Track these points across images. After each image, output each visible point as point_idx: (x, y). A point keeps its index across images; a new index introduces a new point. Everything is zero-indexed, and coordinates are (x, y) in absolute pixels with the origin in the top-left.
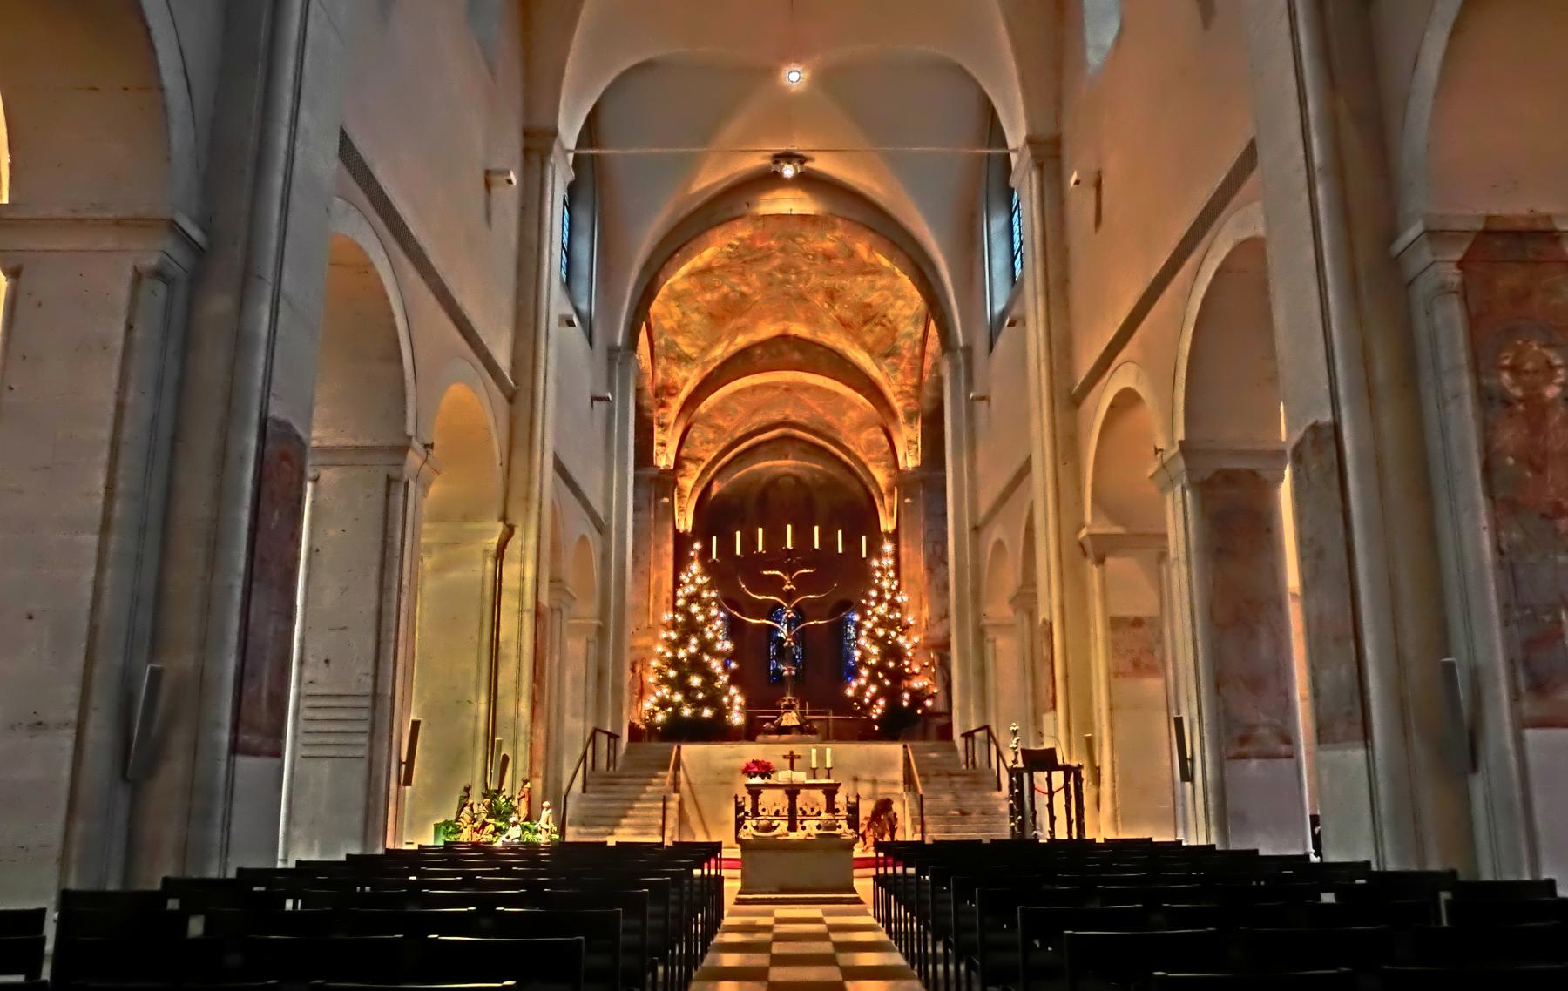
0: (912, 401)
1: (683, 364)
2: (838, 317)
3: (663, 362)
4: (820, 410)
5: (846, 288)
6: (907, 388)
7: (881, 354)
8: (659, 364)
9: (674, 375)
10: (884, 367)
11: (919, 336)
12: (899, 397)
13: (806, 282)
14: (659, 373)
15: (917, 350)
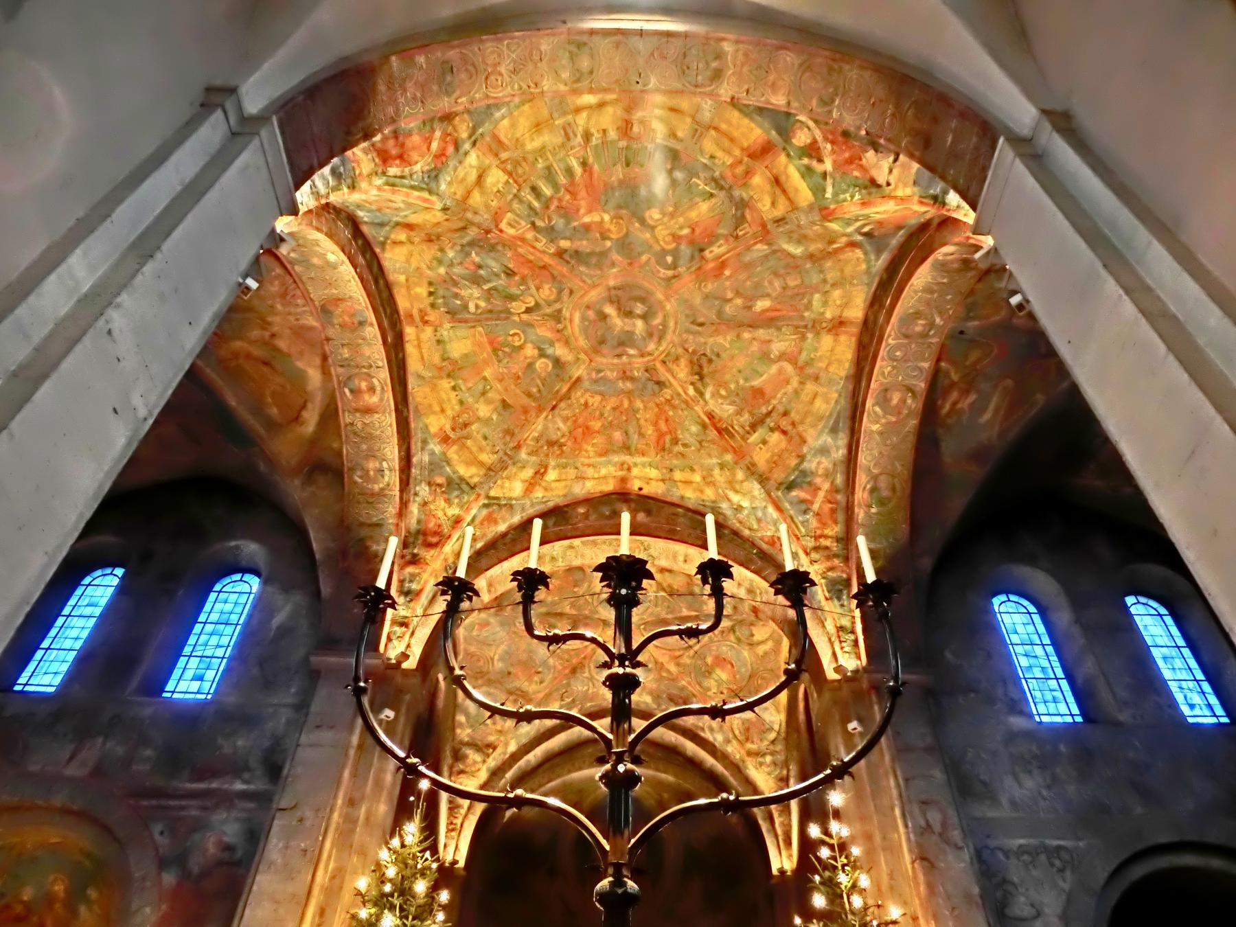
0: (836, 562)
1: (456, 493)
2: (711, 416)
3: (423, 490)
4: (672, 668)
5: (724, 355)
6: (827, 543)
7: (781, 484)
8: (416, 494)
9: (440, 514)
10: (787, 505)
11: (840, 453)
12: (814, 556)
13: (660, 339)
14: (414, 509)
15: (839, 480)
